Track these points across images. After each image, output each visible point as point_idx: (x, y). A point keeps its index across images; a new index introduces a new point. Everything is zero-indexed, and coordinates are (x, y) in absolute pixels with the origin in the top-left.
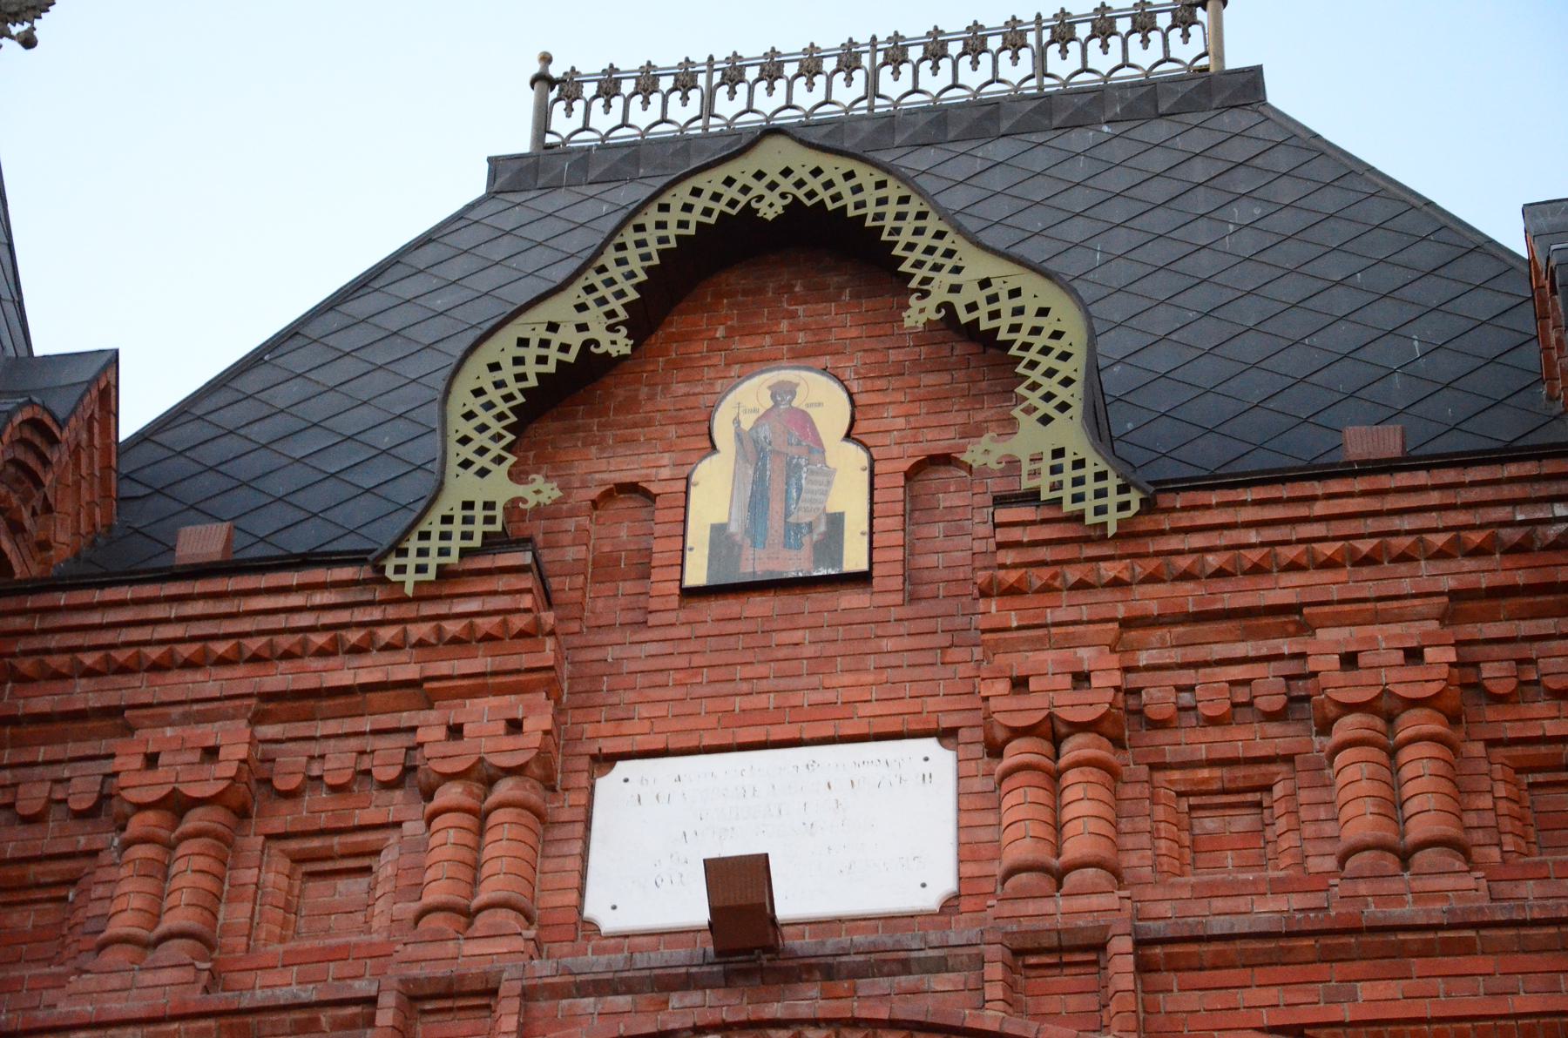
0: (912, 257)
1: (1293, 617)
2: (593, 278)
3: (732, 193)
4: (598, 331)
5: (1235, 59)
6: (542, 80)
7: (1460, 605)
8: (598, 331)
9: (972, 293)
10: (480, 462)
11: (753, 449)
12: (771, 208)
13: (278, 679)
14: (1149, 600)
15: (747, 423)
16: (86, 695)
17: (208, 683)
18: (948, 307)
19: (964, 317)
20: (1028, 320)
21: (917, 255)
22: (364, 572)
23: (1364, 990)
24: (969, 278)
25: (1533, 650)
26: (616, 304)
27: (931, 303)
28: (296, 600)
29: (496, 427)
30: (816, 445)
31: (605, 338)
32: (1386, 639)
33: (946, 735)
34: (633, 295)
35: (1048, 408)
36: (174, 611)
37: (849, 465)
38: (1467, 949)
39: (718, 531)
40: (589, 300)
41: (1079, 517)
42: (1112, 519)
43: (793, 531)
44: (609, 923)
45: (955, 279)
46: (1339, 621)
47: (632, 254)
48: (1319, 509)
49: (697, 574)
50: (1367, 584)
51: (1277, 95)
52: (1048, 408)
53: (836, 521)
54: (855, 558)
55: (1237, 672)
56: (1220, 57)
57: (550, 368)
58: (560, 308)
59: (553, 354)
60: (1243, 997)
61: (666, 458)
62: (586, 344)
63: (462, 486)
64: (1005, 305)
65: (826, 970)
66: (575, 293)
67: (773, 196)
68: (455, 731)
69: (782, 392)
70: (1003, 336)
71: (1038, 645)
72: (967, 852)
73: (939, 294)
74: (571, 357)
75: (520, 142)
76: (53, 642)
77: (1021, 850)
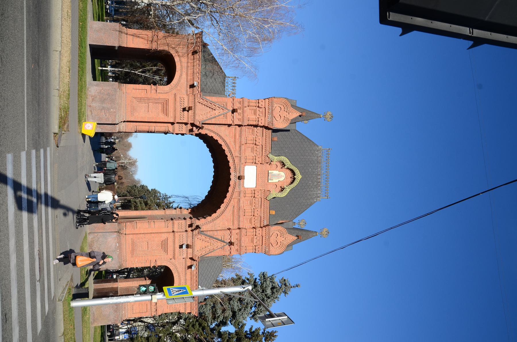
2: (291, 165)
3: (297, 174)
4: (287, 166)
8: (287, 166)
10: (277, 159)
11: (279, 175)
12: (295, 177)
15: (281, 174)
16: (264, 134)
19: (284, 189)
22: (270, 152)
24: (288, 189)
25: (257, 220)
26: (289, 167)
27: (286, 187)
28: (269, 148)
29: (280, 160)
30: (278, 178)
34: (290, 168)
35: (276, 195)
36: (269, 140)
37: (277, 181)
38: (238, 216)
39: (273, 172)
40: (290, 165)
41: (268, 196)
44: (245, 167)
45: (288, 189)
46: (260, 210)
47: (293, 168)
48: (267, 209)
49: (269, 171)
52: (276, 195)
53: (273, 180)
54: (269, 181)
55: (258, 204)
57: (284, 163)
59: (285, 163)
60: (236, 204)
61: (279, 169)
62: (286, 165)
64: (285, 192)
70: (283, 192)
71: (261, 193)
72: (247, 188)
74: (285, 164)
76: (268, 133)
77: (247, 192)
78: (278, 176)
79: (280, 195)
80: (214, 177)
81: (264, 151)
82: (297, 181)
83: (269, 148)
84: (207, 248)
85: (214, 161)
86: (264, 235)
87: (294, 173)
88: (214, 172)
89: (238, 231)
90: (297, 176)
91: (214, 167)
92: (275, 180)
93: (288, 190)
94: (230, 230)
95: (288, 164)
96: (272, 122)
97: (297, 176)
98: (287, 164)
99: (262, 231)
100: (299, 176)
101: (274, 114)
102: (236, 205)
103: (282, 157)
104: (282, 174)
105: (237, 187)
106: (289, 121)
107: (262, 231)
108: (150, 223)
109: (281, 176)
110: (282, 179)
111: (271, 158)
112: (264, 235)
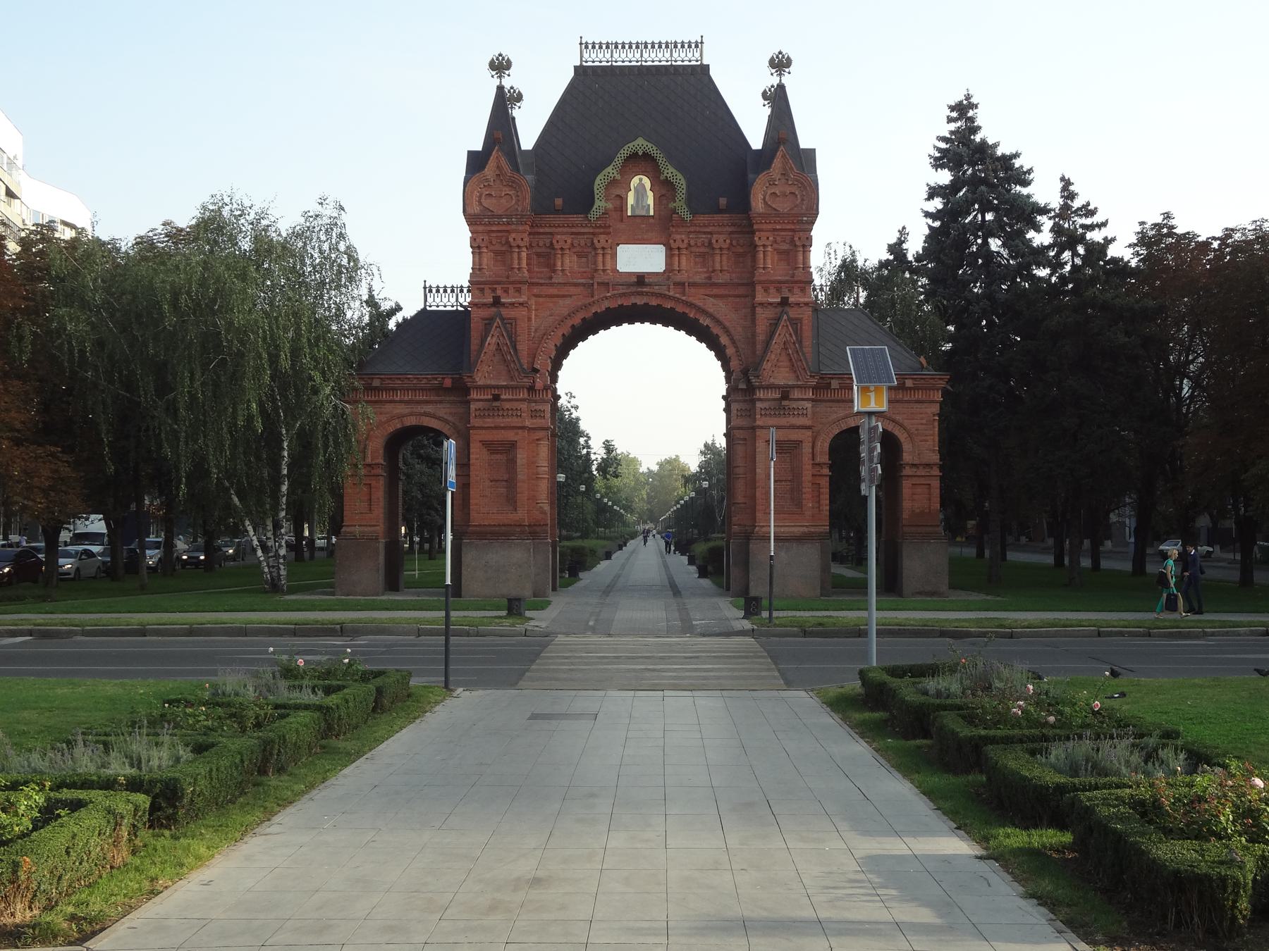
0: (662, 165)
1: (711, 233)
5: (705, 62)
6: (581, 44)
7: (731, 233)
8: (615, 174)
9: (670, 175)
13: (574, 230)
14: (692, 229)
17: (565, 230)
18: (666, 177)
20: (678, 181)
21: (662, 165)
23: (715, 290)
31: (617, 176)
32: (721, 238)
33: (664, 245)
35: (680, 198)
37: (650, 195)
42: (688, 219)
43: (643, 207)
45: (667, 171)
49: (629, 214)
50: (720, 229)
51: (712, 73)
53: (649, 205)
56: (701, 60)
58: (609, 169)
62: (614, 177)
63: (597, 203)
65: (650, 285)
66: (611, 167)
67: (640, 150)
68: (599, 241)
69: (641, 180)
73: (665, 174)
75: (578, 64)
78: (640, 191)
79: (680, 190)
80: (654, 322)
81: (583, 230)
82: (651, 149)
83: (578, 219)
84: (792, 356)
85: (619, 324)
86: (770, 227)
87: (633, 157)
88: (642, 322)
89: (759, 288)
90: (638, 148)
91: (631, 322)
92: (650, 201)
93: (671, 169)
94: (755, 305)
95: (611, 171)
96: (519, 217)
97: (638, 148)
98: (610, 175)
99: (759, 230)
100: (640, 144)
101: (500, 213)
102: (702, 291)
103: (595, 189)
104: (635, 181)
105: (664, 290)
106: (515, 176)
107: (759, 230)
108: (736, 474)
109: (641, 185)
110: (647, 182)
111: (598, 214)
112: (770, 227)
